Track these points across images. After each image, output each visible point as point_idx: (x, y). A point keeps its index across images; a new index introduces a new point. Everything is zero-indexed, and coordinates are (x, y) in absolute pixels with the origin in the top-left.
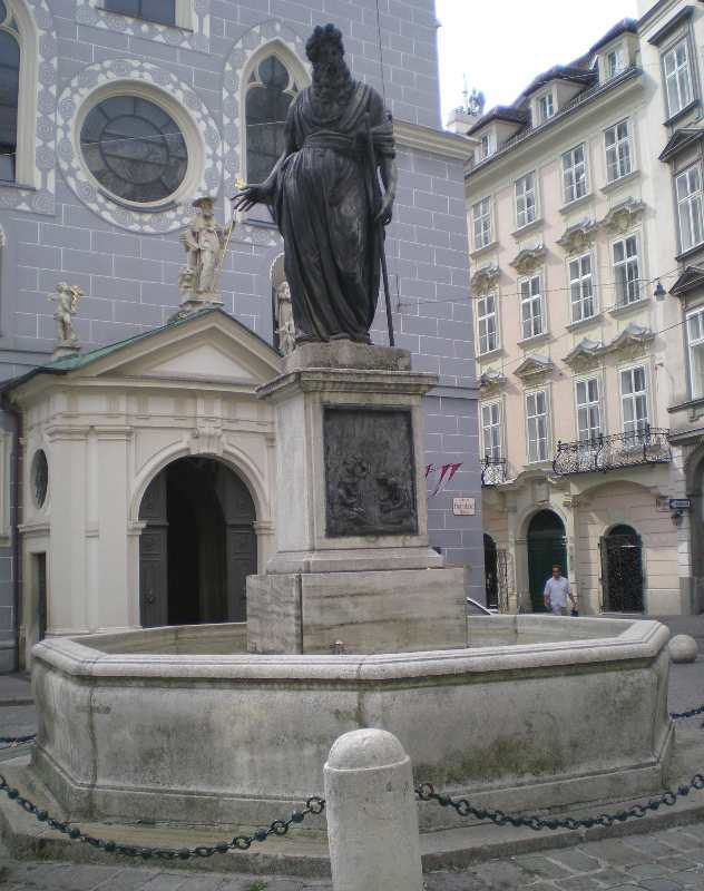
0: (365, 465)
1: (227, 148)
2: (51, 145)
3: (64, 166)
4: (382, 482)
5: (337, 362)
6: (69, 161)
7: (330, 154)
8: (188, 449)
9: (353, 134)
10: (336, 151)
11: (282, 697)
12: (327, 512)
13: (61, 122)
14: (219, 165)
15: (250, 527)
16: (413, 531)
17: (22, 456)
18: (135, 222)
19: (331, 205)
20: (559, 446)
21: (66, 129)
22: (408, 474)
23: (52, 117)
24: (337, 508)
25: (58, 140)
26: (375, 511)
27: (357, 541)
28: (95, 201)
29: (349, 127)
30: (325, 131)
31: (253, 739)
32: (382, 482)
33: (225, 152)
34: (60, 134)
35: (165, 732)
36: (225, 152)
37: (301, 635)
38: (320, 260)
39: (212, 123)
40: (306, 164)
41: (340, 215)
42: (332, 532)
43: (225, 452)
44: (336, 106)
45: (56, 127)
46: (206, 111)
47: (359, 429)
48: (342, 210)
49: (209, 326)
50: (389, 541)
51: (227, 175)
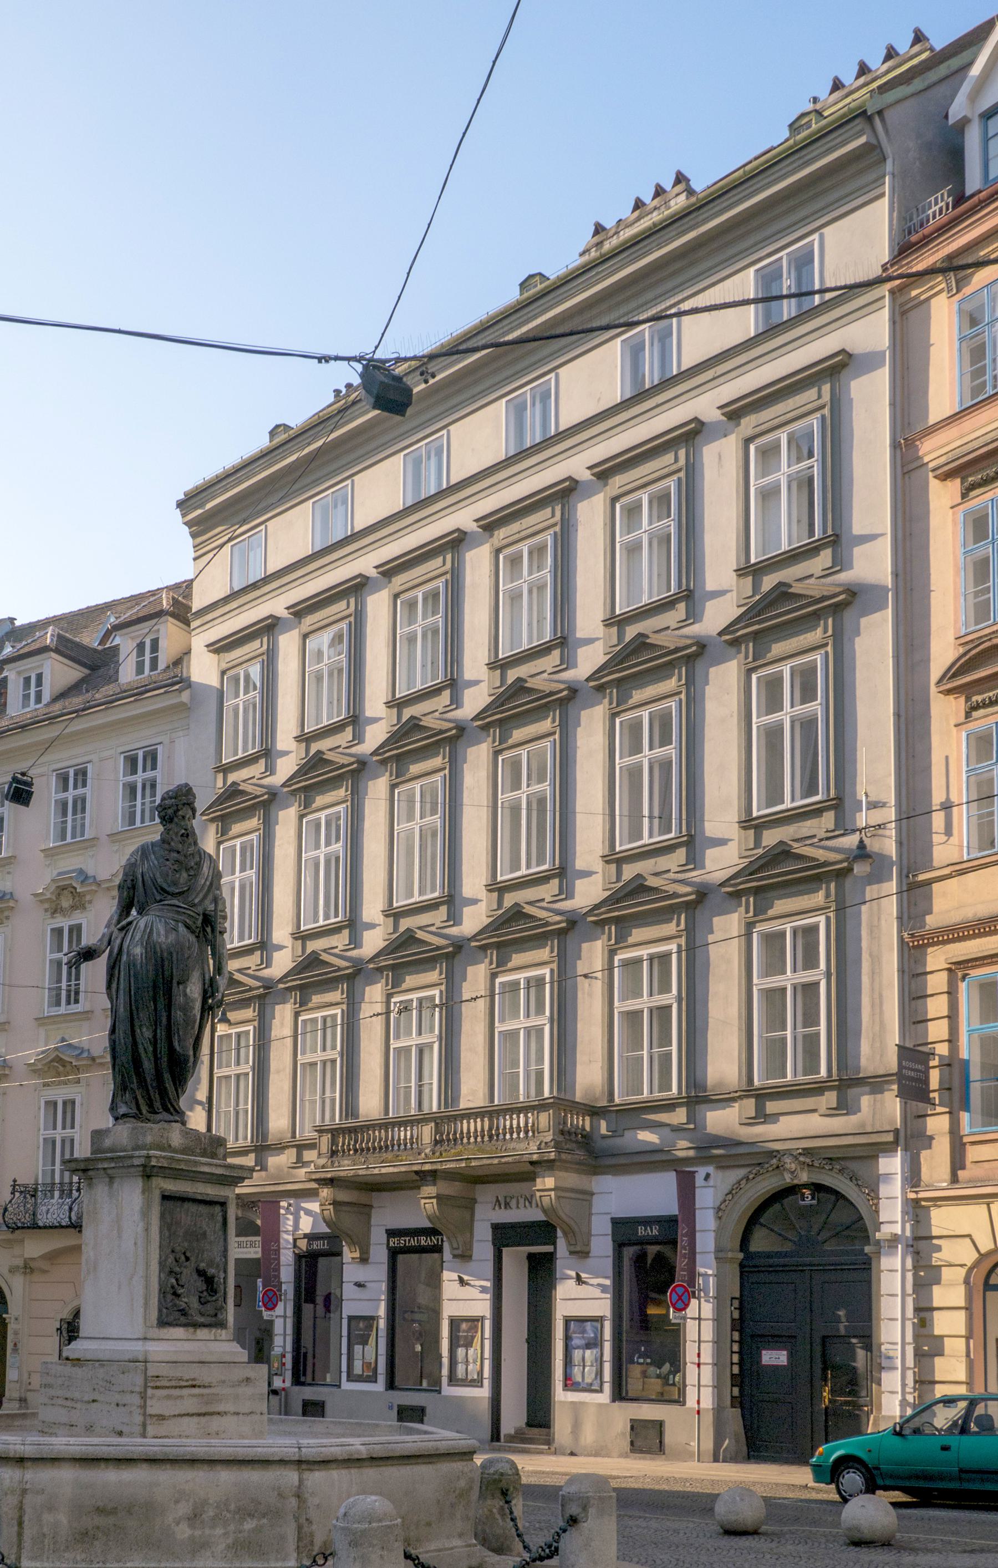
0: (188, 1254)
4: (201, 1273)
5: (170, 1146)
7: (182, 928)
9: (200, 909)
11: (226, 1476)
12: (159, 1301)
16: (222, 1325)
19: (179, 983)
20: (14, 1186)
22: (222, 1266)
24: (170, 1297)
26: (195, 1303)
27: (179, 1332)
29: (196, 901)
30: (175, 902)
31: (195, 1516)
32: (201, 1273)
35: (100, 1511)
37: (144, 1425)
38: (155, 1036)
40: (159, 934)
41: (185, 995)
42: (163, 1323)
44: (185, 875)
47: (187, 1216)
48: (188, 990)
50: (203, 1333)
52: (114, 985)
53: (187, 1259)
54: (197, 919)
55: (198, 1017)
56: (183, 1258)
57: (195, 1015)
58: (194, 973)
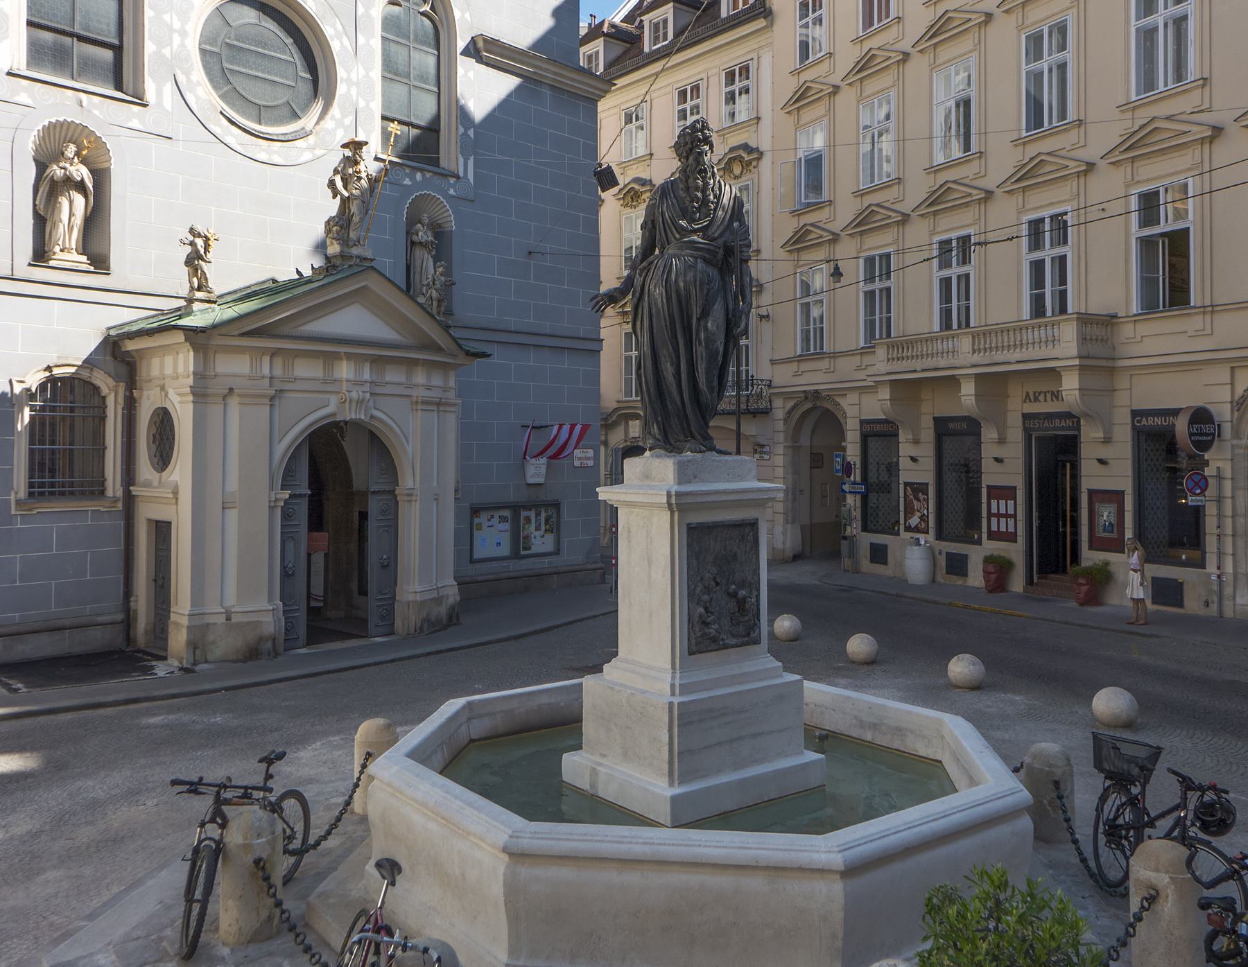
1: (362, 72)
2: (166, 52)
3: (181, 79)
6: (187, 74)
7: (701, 265)
8: (334, 414)
9: (720, 241)
10: (705, 260)
13: (177, 25)
14: (354, 91)
15: (392, 492)
17: (135, 410)
18: (262, 150)
21: (183, 34)
23: (167, 17)
25: (175, 47)
28: (220, 126)
29: (716, 235)
33: (360, 77)
34: (177, 39)
36: (360, 77)
39: (346, 41)
43: (372, 417)
45: (172, 30)
46: (339, 27)
49: (363, 284)
51: (362, 104)
52: (638, 323)
53: (717, 584)
54: (717, 253)
55: (721, 349)
56: (713, 583)
57: (717, 349)
58: (716, 307)
